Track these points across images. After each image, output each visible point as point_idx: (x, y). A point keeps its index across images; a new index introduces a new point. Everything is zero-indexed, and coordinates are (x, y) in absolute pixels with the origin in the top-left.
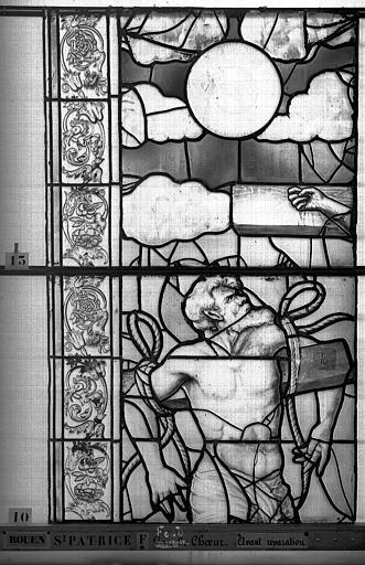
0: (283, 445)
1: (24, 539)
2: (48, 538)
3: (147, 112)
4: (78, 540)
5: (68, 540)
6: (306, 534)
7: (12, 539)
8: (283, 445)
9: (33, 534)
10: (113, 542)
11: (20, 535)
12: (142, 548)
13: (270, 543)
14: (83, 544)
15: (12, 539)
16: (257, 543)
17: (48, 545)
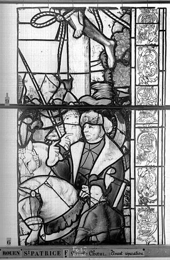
1: (10, 253)
2: (21, 252)
4: (35, 253)
5: (31, 253)
6: (144, 250)
7: (4, 253)
10: (52, 253)
11: (7, 253)
12: (66, 257)
13: (126, 254)
15: (4, 253)
16: (120, 254)
17: (21, 256)
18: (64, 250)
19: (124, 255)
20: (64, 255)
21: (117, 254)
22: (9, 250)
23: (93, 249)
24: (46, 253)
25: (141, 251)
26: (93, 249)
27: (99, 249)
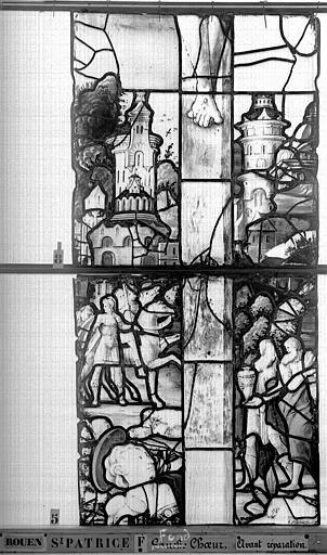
0: (290, 439)
2: (45, 541)
3: (236, 51)
4: (75, 542)
5: (65, 543)
6: (307, 537)
7: (9, 542)
8: (290, 439)
9: (28, 536)
11: (15, 539)
12: (140, 550)
14: (81, 546)
18: (136, 537)
19: (264, 547)
20: (137, 548)
21: (248, 545)
22: (19, 536)
23: (198, 534)
24: (99, 543)
25: (301, 539)
26: (198, 534)
27: (211, 534)
